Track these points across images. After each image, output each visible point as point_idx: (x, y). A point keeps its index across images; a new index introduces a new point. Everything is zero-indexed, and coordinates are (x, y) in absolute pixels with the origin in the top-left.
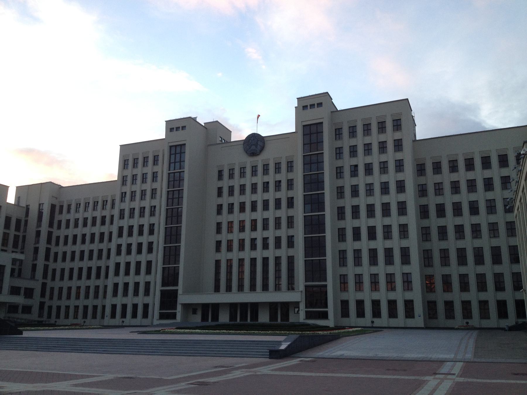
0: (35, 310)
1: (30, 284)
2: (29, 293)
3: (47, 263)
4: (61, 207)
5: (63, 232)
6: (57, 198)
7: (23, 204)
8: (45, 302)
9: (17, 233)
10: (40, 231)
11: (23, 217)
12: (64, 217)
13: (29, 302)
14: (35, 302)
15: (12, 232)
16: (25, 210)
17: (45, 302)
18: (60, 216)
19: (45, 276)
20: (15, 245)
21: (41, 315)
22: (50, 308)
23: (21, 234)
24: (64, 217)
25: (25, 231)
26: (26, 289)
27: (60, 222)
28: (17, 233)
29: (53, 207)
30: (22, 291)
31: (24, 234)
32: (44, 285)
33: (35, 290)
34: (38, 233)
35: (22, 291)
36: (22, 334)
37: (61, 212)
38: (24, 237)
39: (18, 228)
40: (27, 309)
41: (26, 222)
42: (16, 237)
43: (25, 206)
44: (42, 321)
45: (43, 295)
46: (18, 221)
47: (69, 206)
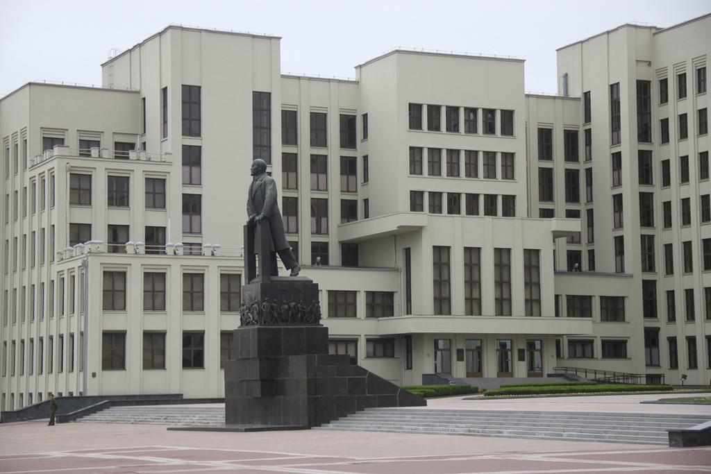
0: (637, 347)
1: (612, 288)
2: (613, 308)
3: (647, 231)
4: (664, 83)
5: (673, 151)
6: (649, 63)
7: (576, 92)
8: (657, 330)
9: (572, 166)
10: (619, 153)
11: (577, 122)
12: (672, 110)
13: (613, 330)
14: (632, 328)
15: (559, 165)
16: (582, 103)
17: (657, 330)
18: (664, 107)
19: (648, 264)
20: (572, 195)
21: (652, 361)
22: (673, 341)
23: (581, 166)
24: (672, 110)
25: (589, 158)
26: (604, 299)
27: (665, 123)
28: (572, 166)
29: (643, 88)
30: (596, 306)
31: (588, 166)
32: (649, 289)
33: (626, 300)
34: (617, 158)
35: (596, 306)
36: (425, 404)
37: (664, 98)
38: (589, 172)
39: (571, 154)
40: (616, 349)
41: (588, 133)
42: (572, 177)
43: (579, 94)
44: (659, 376)
45: (650, 309)
46: (571, 137)
47: (682, 78)
